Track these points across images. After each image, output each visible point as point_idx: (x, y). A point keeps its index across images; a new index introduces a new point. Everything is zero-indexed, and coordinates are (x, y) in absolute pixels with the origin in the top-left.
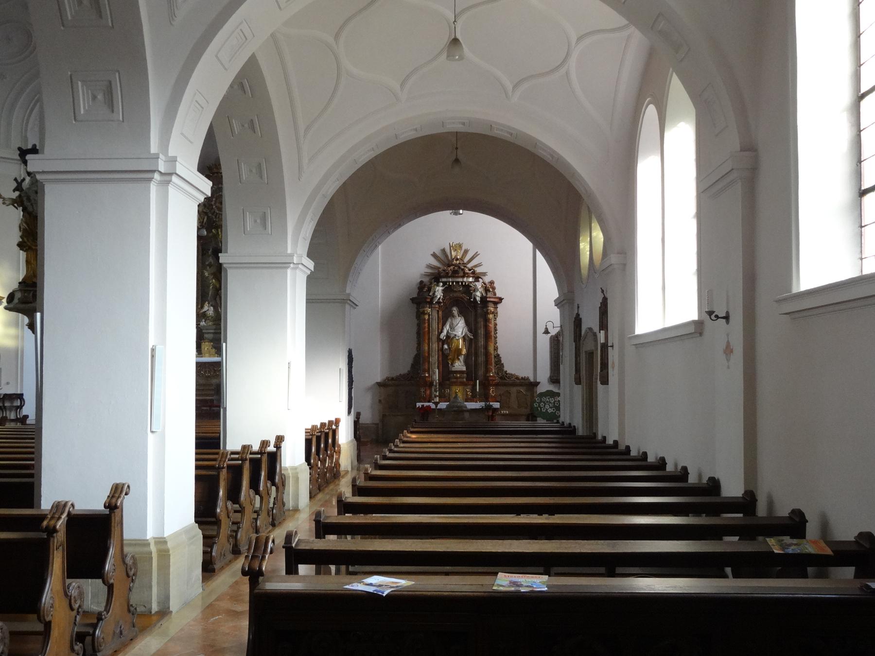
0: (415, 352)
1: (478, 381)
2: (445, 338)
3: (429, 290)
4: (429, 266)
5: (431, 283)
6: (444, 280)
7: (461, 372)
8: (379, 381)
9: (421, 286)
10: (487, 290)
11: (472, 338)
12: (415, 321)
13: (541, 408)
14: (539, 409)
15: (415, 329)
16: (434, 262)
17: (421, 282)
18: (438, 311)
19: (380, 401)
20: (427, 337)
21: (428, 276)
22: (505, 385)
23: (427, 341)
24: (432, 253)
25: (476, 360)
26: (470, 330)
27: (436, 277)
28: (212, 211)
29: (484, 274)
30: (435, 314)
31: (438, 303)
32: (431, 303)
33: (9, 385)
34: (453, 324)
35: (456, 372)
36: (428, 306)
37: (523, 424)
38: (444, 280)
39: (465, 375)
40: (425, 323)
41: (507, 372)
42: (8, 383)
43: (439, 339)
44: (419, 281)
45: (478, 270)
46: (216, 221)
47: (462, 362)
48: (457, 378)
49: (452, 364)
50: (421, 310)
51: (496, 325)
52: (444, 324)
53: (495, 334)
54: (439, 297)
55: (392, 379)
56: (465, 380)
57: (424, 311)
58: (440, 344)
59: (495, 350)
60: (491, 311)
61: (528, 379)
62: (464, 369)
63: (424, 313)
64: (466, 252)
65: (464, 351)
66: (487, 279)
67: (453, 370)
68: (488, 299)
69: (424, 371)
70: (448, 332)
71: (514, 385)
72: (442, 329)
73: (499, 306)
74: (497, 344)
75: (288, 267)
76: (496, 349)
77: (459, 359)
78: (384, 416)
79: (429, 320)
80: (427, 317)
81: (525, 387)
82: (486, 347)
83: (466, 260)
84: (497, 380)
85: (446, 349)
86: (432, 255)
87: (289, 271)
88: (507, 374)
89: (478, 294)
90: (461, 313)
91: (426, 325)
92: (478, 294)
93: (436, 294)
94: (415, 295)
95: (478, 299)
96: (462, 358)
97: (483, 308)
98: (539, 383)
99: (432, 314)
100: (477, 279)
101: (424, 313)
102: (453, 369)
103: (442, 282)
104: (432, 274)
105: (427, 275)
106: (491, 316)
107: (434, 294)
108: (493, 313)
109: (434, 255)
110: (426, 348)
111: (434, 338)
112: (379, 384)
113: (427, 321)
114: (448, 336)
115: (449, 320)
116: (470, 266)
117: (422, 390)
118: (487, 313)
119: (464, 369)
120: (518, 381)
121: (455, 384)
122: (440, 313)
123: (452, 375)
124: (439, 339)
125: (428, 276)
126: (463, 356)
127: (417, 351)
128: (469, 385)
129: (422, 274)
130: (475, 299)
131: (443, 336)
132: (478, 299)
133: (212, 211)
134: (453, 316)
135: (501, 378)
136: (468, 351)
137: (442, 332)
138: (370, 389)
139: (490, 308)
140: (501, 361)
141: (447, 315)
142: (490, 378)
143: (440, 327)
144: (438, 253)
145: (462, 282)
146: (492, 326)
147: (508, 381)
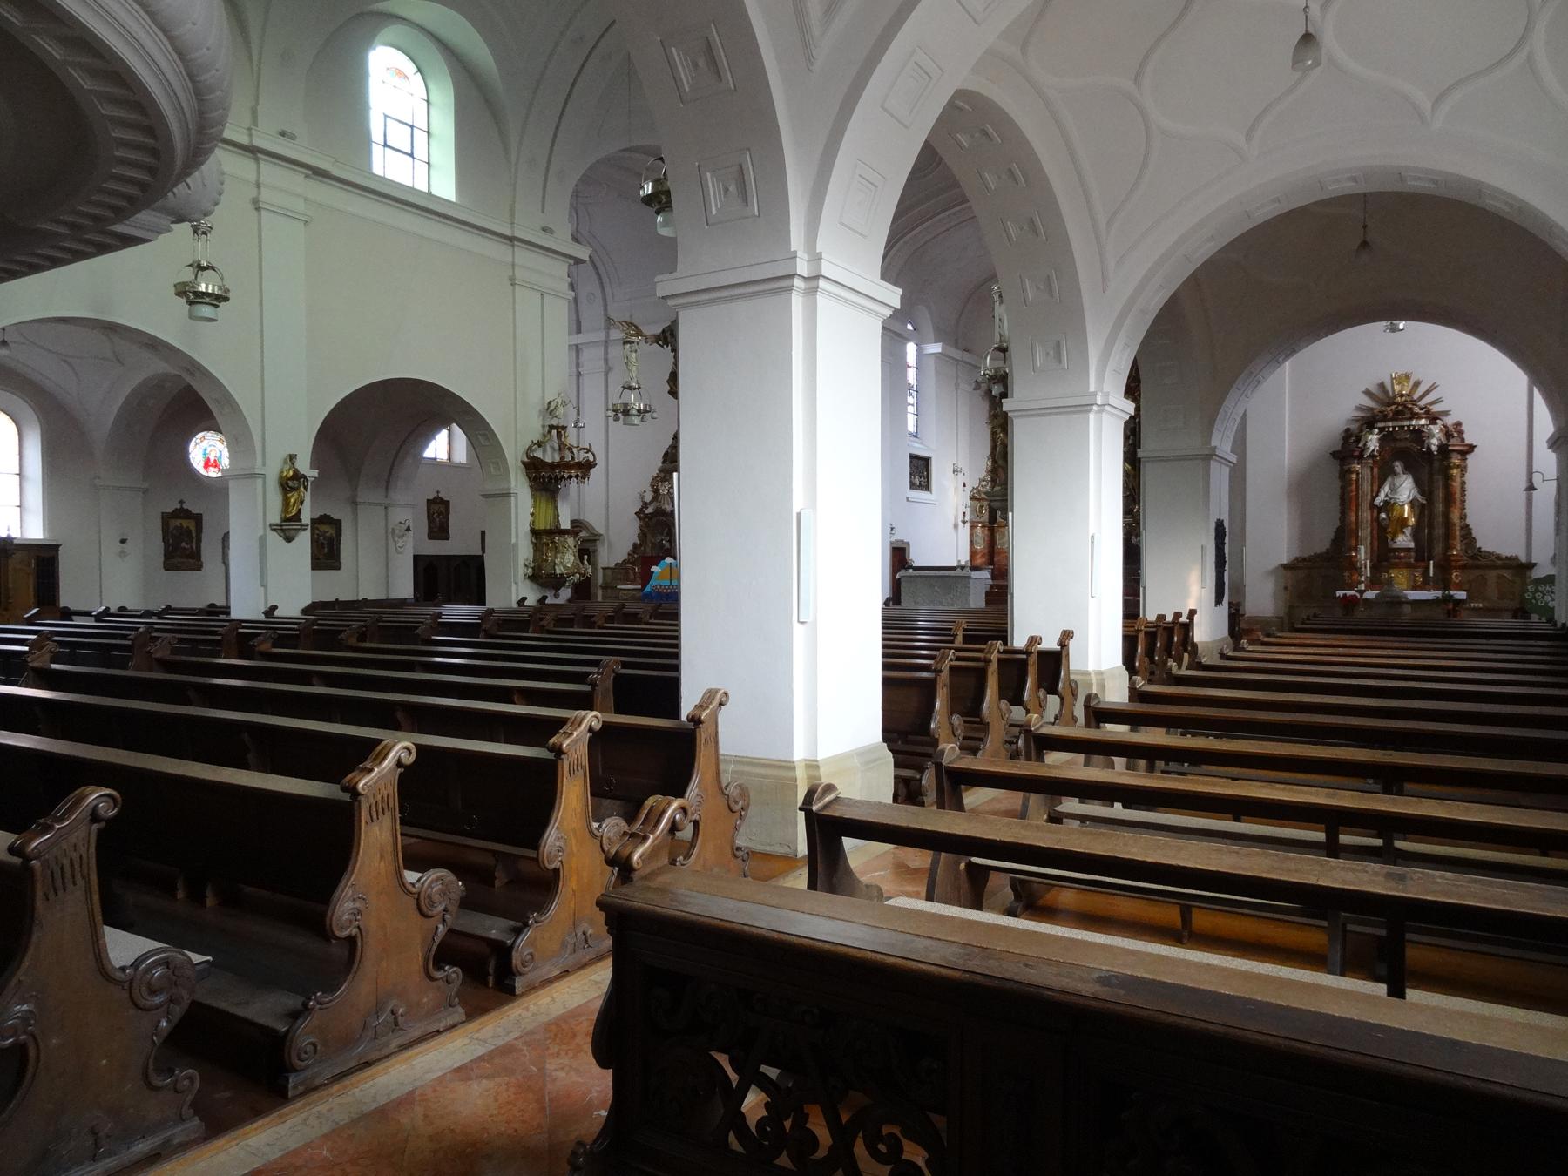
0: (1338, 524)
1: (1432, 562)
2: (1382, 504)
3: (1358, 440)
4: (1360, 408)
5: (1362, 431)
6: (1381, 425)
7: (1408, 550)
8: (1285, 562)
9: (1347, 434)
10: (1448, 435)
11: (1424, 502)
12: (1337, 484)
13: (1537, 600)
14: (1534, 601)
15: (1338, 491)
16: (1368, 402)
17: (1348, 430)
18: (1372, 469)
19: (1286, 588)
20: (1354, 504)
22: (1478, 567)
23: (1354, 508)
24: (1364, 389)
25: (1430, 534)
26: (1422, 492)
27: (1369, 422)
29: (1446, 413)
30: (1367, 472)
31: (1372, 456)
32: (1360, 457)
34: (1394, 485)
37: (1506, 623)
38: (1381, 425)
39: (1413, 554)
40: (1351, 485)
41: (1482, 549)
43: (1373, 506)
45: (1435, 408)
47: (1408, 535)
48: (1399, 558)
49: (1392, 540)
50: (1346, 468)
51: (1463, 483)
52: (1381, 485)
53: (1462, 496)
54: (1372, 448)
55: (1304, 560)
56: (1412, 560)
57: (1349, 469)
58: (1375, 512)
59: (1461, 518)
60: (1455, 465)
61: (1516, 558)
62: (1412, 545)
63: (1350, 472)
64: (1417, 384)
65: (1412, 521)
66: (1450, 421)
68: (1450, 448)
69: (1351, 549)
70: (1386, 496)
71: (1493, 567)
72: (1379, 492)
73: (1470, 457)
74: (1466, 511)
75: (1089, 411)
76: (1463, 517)
77: (1404, 533)
78: (1291, 607)
79: (1357, 480)
80: (1354, 476)
81: (1510, 571)
82: (1446, 515)
83: (1416, 397)
84: (1465, 560)
85: (1384, 519)
86: (1364, 392)
87: (1092, 416)
88: (1481, 552)
89: (1435, 441)
90: (1408, 469)
91: (1354, 486)
92: (1435, 441)
93: (1369, 444)
94: (1338, 448)
95: (1434, 448)
96: (1408, 531)
97: (1442, 460)
98: (1535, 564)
99: (1362, 472)
100: (1433, 419)
101: (1350, 472)
102: (1395, 546)
103: (1379, 428)
105: (1356, 420)
106: (1455, 471)
107: (1365, 445)
108: (1458, 467)
109: (1368, 393)
110: (1353, 519)
111: (1365, 506)
112: (1285, 567)
113: (1354, 482)
114: (1386, 502)
115: (1390, 479)
116: (1422, 403)
117: (1346, 574)
118: (1449, 467)
119: (1412, 545)
120: (1499, 562)
121: (1396, 566)
122: (1376, 470)
123: (1392, 554)
124: (1373, 506)
125: (1357, 421)
126: (1409, 528)
127: (1341, 522)
128: (1419, 567)
129: (1348, 420)
130: (1429, 448)
131: (1379, 501)
132: (1434, 448)
134: (1394, 474)
135: (1471, 558)
136: (1419, 522)
137: (1377, 495)
138: (1274, 571)
139: (1453, 460)
140: (1471, 534)
141: (1384, 473)
142: (1453, 558)
143: (1375, 488)
144: (1374, 389)
145: (1409, 427)
146: (1456, 485)
147: (1483, 561)
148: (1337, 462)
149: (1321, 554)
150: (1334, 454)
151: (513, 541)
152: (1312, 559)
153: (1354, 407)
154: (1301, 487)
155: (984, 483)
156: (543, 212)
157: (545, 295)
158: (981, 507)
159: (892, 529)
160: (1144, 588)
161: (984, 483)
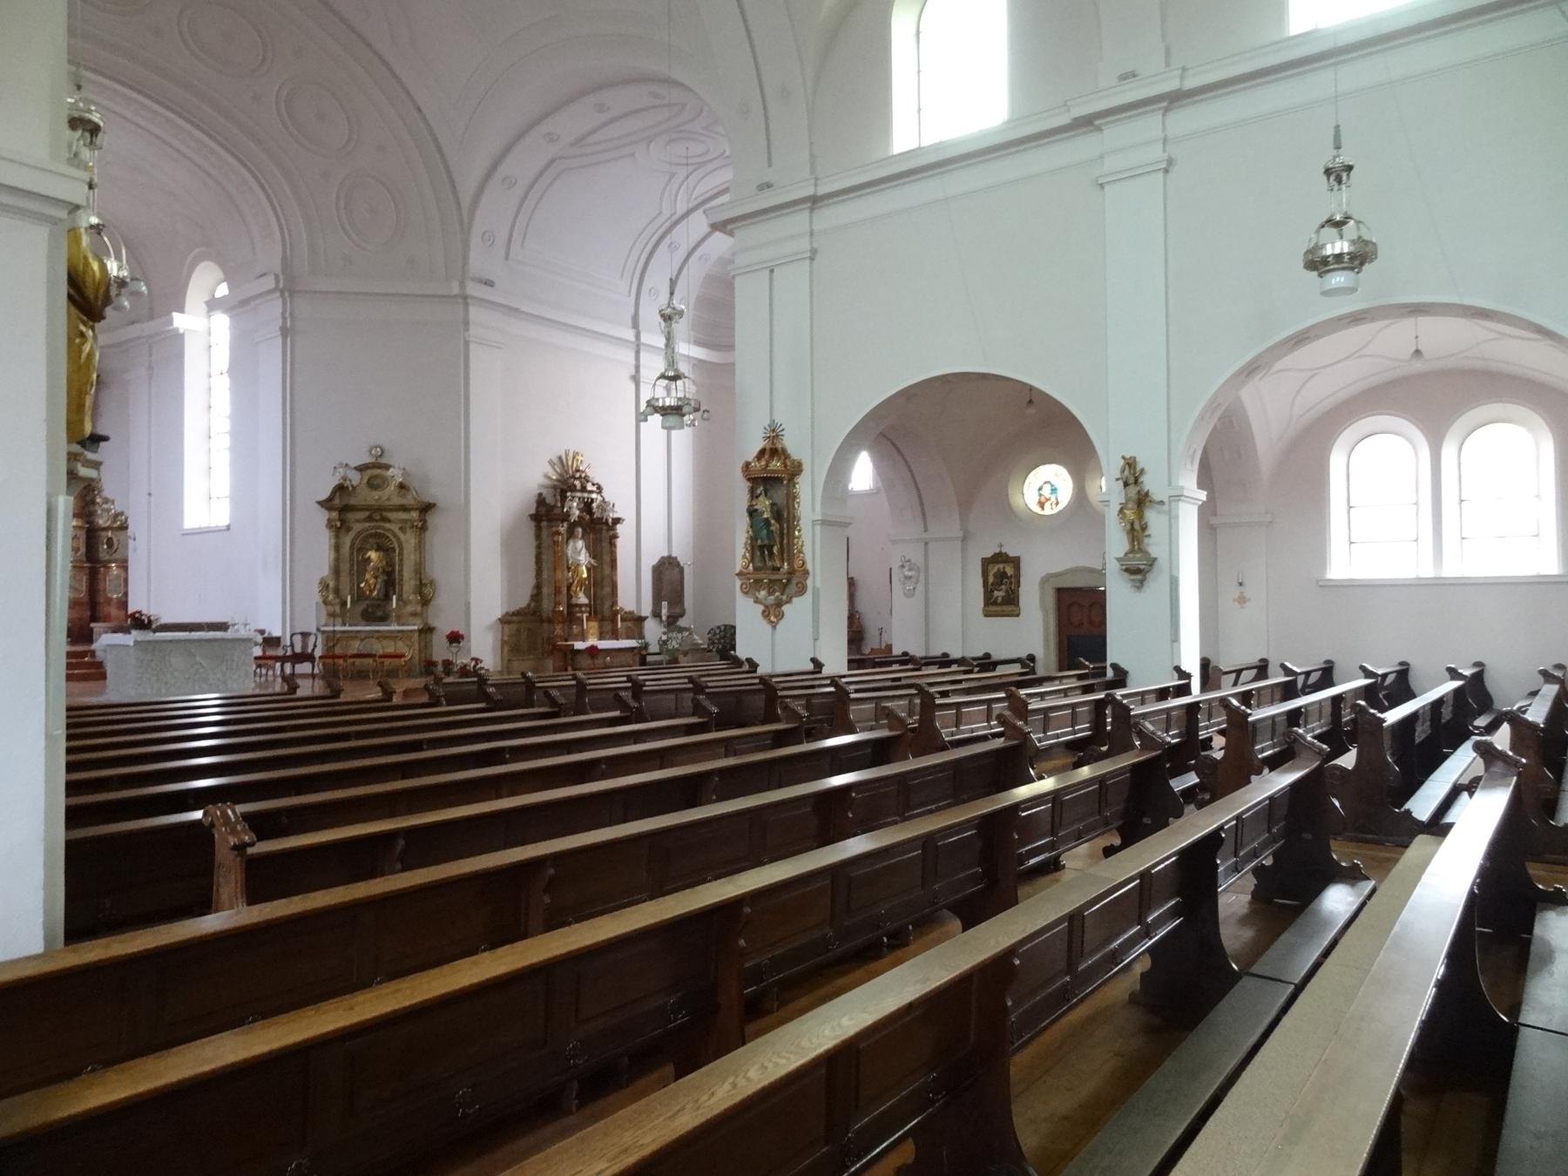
0: (532, 582)
7: (586, 605)
9: (541, 501)
12: (533, 543)
17: (540, 495)
19: (503, 643)
34: (576, 548)
35: (581, 606)
44: (538, 492)
78: (509, 660)
94: (533, 511)
104: (555, 487)
109: (551, 463)
112: (505, 620)
134: (576, 537)
138: (490, 628)
141: (571, 534)
149: (525, 608)
152: (518, 613)
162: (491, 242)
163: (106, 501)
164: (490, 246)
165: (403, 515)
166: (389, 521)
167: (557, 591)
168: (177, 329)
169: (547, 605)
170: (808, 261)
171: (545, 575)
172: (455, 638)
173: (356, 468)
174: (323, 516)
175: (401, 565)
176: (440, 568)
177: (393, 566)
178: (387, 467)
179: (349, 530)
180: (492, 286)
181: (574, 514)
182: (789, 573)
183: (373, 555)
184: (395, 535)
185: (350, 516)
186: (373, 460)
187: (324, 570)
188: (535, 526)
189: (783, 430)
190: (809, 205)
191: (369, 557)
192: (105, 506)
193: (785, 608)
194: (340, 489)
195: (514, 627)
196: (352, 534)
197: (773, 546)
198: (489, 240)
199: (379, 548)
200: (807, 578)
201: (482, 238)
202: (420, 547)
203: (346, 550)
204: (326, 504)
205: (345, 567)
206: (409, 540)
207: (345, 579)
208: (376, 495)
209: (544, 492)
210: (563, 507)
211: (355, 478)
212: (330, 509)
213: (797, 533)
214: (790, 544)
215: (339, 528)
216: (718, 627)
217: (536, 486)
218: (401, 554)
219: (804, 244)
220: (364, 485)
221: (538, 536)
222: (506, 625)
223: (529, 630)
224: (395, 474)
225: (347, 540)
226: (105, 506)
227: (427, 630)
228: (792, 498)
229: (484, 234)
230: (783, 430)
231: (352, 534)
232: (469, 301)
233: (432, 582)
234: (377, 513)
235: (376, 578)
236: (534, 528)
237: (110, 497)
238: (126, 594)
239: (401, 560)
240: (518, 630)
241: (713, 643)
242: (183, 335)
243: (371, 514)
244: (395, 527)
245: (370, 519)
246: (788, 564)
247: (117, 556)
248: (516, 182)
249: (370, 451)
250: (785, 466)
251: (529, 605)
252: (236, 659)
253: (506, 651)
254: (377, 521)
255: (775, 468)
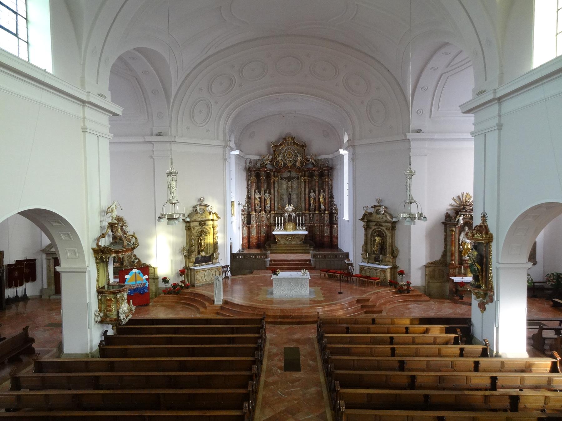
0: (443, 249)
4: (451, 205)
8: (425, 264)
9: (448, 216)
12: (444, 234)
15: (443, 237)
16: (453, 203)
17: (447, 213)
19: (426, 275)
21: (450, 210)
27: (457, 212)
28: (285, 159)
33: (222, 260)
36: (454, 227)
42: (221, 260)
46: (287, 164)
55: (432, 263)
67: (465, 259)
70: (462, 239)
78: (429, 282)
80: (453, 233)
94: (443, 221)
99: (456, 230)
104: (455, 209)
105: (449, 210)
109: (454, 199)
112: (426, 266)
114: (462, 242)
125: (450, 210)
127: (445, 249)
133: (285, 159)
138: (420, 268)
144: (456, 198)
148: (444, 225)
149: (438, 261)
150: (443, 223)
151: (88, 301)
153: (449, 205)
154: (430, 235)
155: (245, 207)
156: (97, 84)
157: (100, 137)
158: (244, 217)
159: (230, 239)
160: (497, 329)
161: (245, 207)
162: (421, 114)
163: (335, 205)
164: (421, 115)
165: (387, 224)
166: (382, 226)
167: (452, 255)
168: (342, 154)
169: (448, 259)
170: (497, 131)
171: (448, 247)
172: (402, 273)
173: (371, 207)
174: (362, 223)
175: (386, 243)
176: (400, 244)
177: (384, 242)
178: (380, 206)
179: (371, 228)
180: (419, 132)
181: (460, 222)
182: (484, 290)
183: (377, 239)
184: (385, 232)
185: (371, 224)
186: (377, 204)
187: (362, 243)
188: (445, 227)
189: (487, 217)
190: (496, 101)
191: (376, 239)
192: (335, 207)
193: (486, 306)
194: (365, 215)
195: (431, 269)
196: (371, 230)
197: (478, 276)
198: (420, 113)
199: (379, 236)
200: (493, 295)
201: (417, 113)
202: (393, 236)
203: (369, 235)
204: (362, 219)
205: (369, 242)
206: (388, 234)
207: (369, 247)
208: (378, 216)
209: (449, 212)
210: (455, 219)
211: (371, 210)
212: (364, 222)
213: (490, 271)
214: (487, 276)
215: (367, 227)
216: (553, 274)
217: (445, 210)
218: (386, 238)
219: (496, 121)
220: (375, 213)
221: (445, 231)
222: (427, 268)
223: (440, 270)
224: (382, 210)
225: (370, 232)
226: (335, 207)
227: (394, 268)
228: (488, 253)
229: (417, 112)
230: (487, 217)
231: (371, 230)
232: (410, 140)
233: (397, 250)
234: (378, 224)
235: (377, 247)
236: (444, 228)
237: (336, 204)
238: (338, 235)
239: (386, 241)
240: (434, 270)
241: (549, 281)
242: (344, 155)
243: (376, 224)
244: (384, 228)
245: (376, 225)
246: (486, 286)
247: (337, 222)
248: (427, 88)
249: (377, 200)
250: (483, 238)
251: (440, 259)
252: (303, 284)
253: (427, 278)
254: (378, 226)
255: (478, 238)
